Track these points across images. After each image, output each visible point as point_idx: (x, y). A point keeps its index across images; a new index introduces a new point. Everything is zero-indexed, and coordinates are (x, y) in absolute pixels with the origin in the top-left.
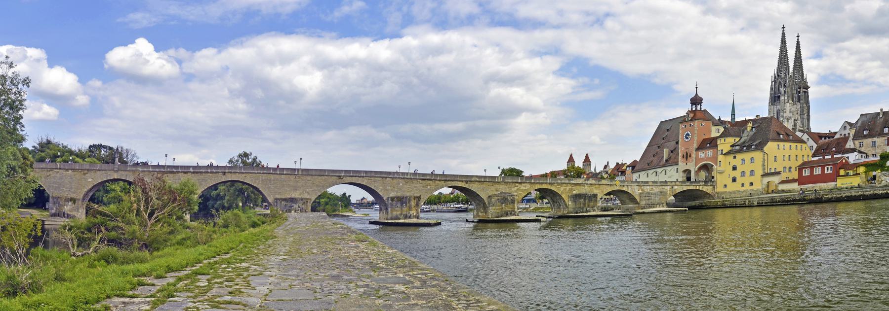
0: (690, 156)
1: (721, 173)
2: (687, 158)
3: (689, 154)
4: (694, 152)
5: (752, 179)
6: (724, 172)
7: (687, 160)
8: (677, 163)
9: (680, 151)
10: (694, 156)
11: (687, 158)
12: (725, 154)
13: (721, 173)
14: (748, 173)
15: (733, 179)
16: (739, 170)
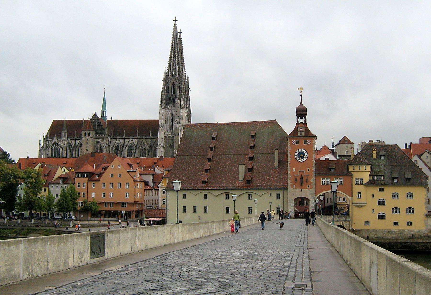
0: (307, 181)
1: (359, 206)
2: (302, 183)
3: (305, 179)
4: (314, 177)
5: (410, 218)
6: (364, 206)
7: (301, 186)
8: (285, 188)
9: (289, 172)
10: (313, 181)
11: (302, 183)
12: (366, 185)
13: (359, 206)
14: (403, 211)
15: (379, 215)
16: (390, 203)
